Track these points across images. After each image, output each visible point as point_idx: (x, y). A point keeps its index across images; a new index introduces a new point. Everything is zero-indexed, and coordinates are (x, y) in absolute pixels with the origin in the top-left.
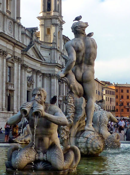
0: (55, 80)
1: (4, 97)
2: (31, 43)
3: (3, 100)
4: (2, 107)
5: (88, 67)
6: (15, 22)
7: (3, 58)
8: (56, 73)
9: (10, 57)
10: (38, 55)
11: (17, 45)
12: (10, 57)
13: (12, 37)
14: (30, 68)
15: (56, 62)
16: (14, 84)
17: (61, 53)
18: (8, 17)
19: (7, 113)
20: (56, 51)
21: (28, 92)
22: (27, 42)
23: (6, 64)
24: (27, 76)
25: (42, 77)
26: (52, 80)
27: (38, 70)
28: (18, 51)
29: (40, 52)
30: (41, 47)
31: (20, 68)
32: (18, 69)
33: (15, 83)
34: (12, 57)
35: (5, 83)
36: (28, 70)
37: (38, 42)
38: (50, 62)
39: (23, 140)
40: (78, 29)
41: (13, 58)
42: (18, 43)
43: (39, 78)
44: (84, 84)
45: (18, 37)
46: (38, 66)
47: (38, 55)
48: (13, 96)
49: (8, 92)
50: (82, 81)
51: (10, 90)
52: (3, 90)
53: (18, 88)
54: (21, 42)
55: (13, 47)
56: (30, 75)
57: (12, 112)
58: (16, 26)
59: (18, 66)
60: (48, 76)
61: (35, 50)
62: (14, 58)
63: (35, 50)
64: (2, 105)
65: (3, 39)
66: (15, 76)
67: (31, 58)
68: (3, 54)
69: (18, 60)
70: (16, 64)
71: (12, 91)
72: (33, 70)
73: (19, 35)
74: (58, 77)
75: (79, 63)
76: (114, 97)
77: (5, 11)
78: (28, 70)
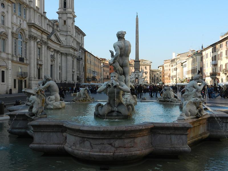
0: (70, 57)
1: (36, 69)
2: (53, 31)
3: (35, 72)
4: (34, 76)
5: (126, 58)
6: (43, 15)
7: (35, 42)
8: (70, 53)
10: (58, 39)
13: (41, 26)
14: (52, 49)
15: (71, 45)
16: (42, 60)
17: (74, 38)
18: (38, 12)
20: (70, 37)
21: (51, 65)
22: (50, 30)
24: (50, 54)
25: (60, 55)
26: (68, 57)
27: (58, 51)
28: (45, 37)
29: (59, 38)
30: (60, 34)
31: (46, 49)
32: (45, 50)
33: (43, 59)
34: (41, 41)
35: (36, 60)
36: (52, 50)
37: (57, 30)
38: (66, 45)
39: (78, 100)
40: (120, 36)
42: (45, 31)
43: (59, 56)
44: (124, 68)
45: (44, 27)
46: (57, 47)
47: (58, 39)
48: (42, 69)
49: (39, 66)
50: (122, 66)
51: (40, 65)
52: (35, 64)
53: (45, 63)
54: (47, 30)
56: (53, 54)
57: (41, 80)
58: (43, 18)
59: (45, 48)
60: (65, 54)
61: (56, 36)
63: (56, 36)
64: (35, 75)
65: (34, 28)
66: (43, 55)
67: (53, 41)
70: (43, 46)
71: (41, 65)
72: (55, 50)
73: (45, 25)
74: (71, 55)
75: (121, 56)
76: (108, 69)
77: (35, 8)
78: (52, 50)
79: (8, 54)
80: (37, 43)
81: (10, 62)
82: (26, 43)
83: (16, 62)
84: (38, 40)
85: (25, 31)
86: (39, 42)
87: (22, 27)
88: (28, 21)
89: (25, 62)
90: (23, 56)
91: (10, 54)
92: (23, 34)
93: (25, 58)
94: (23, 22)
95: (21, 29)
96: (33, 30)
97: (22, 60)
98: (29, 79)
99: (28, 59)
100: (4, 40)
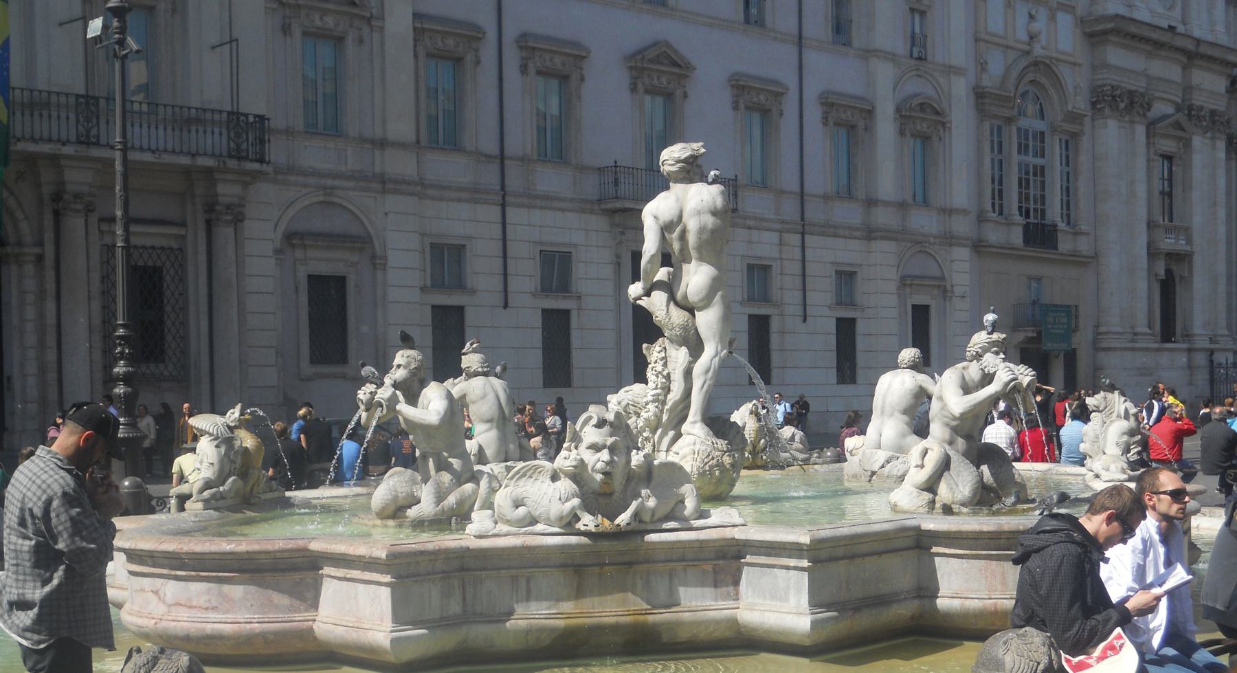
7: (1132, 122)
9: (1170, 110)
11: (1203, 57)
12: (1170, 110)
19: (1157, 350)
23: (1148, 144)
31: (1222, 155)
34: (1178, 108)
41: (1181, 117)
42: (1203, 49)
48: (1188, 280)
51: (1168, 254)
54: (1223, 39)
55: (1185, 68)
57: (1185, 346)
59: (1214, 147)
62: (1189, 115)
68: (1132, 103)
69: (1214, 122)
70: (1197, 141)
71: (1180, 258)
79: (948, 212)
80: (1151, 126)
81: (962, 254)
82: (1075, 135)
83: (1005, 252)
84: (1160, 108)
85: (1065, 72)
86: (1165, 117)
87: (1038, 51)
88: (1079, 12)
89: (1065, 244)
90: (1054, 212)
91: (964, 212)
92: (1052, 91)
93: (1062, 225)
94: (1053, 18)
95: (1036, 64)
96: (1117, 56)
97: (1040, 236)
98: (1095, 341)
99: (1084, 228)
100: (925, 139)
